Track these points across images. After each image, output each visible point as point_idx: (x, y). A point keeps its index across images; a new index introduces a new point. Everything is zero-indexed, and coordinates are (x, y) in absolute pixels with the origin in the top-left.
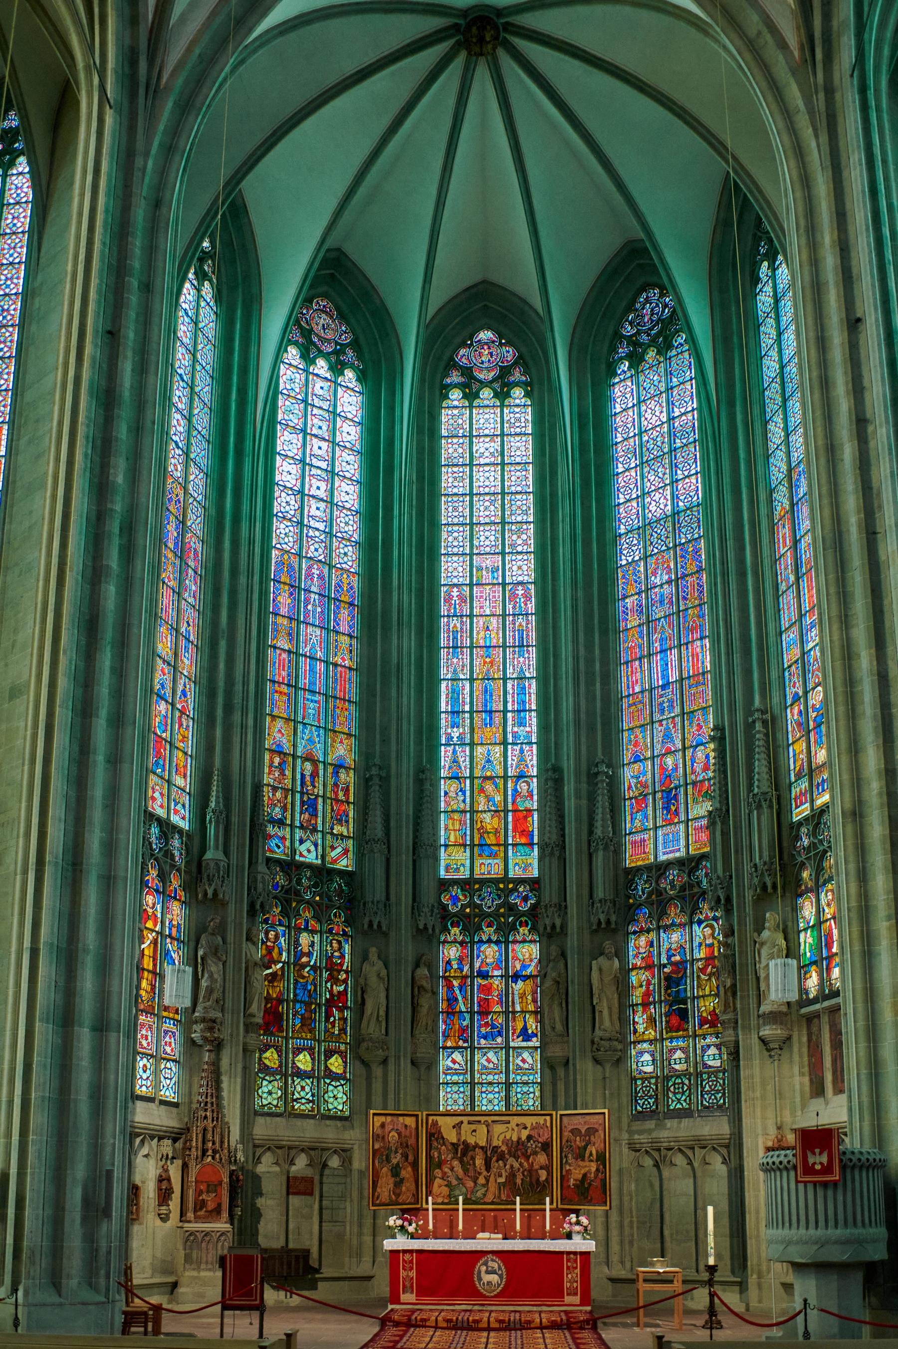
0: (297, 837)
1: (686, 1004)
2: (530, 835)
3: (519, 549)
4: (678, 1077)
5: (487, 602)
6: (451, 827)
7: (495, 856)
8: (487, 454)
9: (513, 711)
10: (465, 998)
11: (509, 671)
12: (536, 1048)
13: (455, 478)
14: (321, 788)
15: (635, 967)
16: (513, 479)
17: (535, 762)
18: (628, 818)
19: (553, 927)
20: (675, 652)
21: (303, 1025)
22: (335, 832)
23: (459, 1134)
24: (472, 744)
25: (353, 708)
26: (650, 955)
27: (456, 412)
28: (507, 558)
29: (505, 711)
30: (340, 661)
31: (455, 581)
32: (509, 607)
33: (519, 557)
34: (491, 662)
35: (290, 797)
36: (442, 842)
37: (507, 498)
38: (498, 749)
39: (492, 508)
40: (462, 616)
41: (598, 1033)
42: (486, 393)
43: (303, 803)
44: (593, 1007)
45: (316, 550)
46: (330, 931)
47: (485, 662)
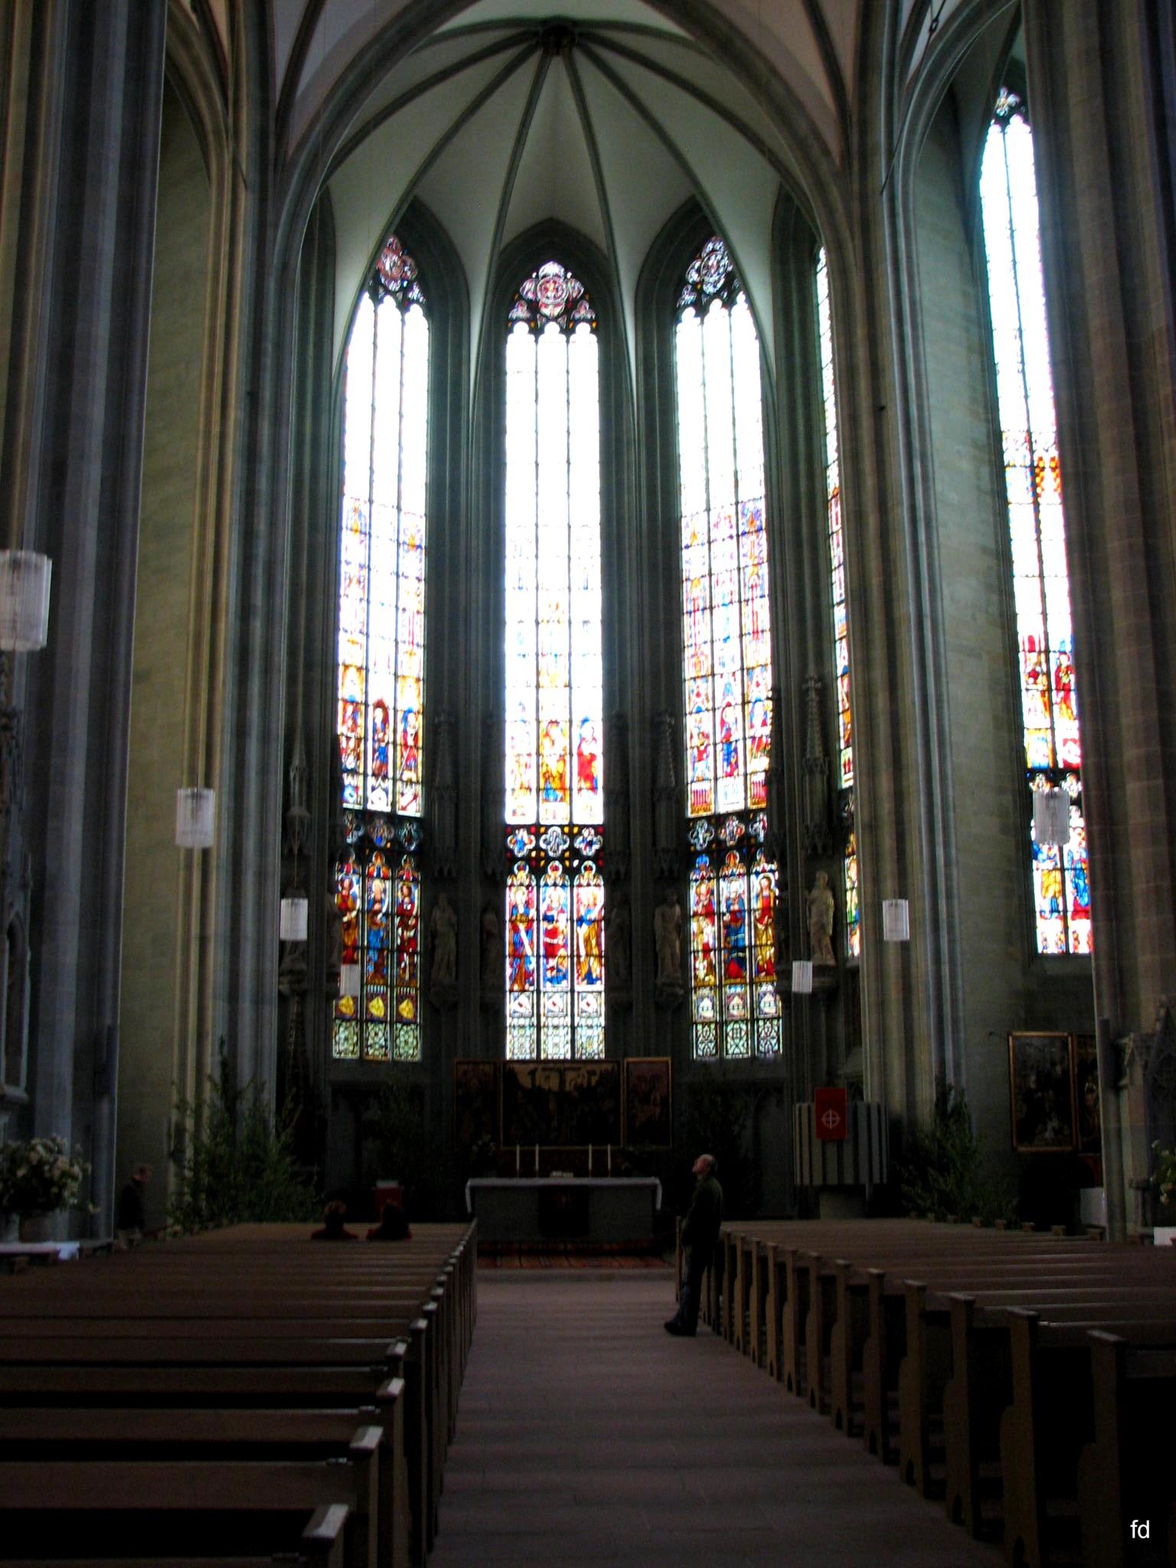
1: (744, 951)
4: (736, 1022)
10: (531, 943)
15: (696, 914)
19: (618, 873)
21: (376, 971)
23: (533, 1080)
26: (710, 903)
41: (659, 981)
42: (552, 329)
44: (656, 955)
46: (401, 878)
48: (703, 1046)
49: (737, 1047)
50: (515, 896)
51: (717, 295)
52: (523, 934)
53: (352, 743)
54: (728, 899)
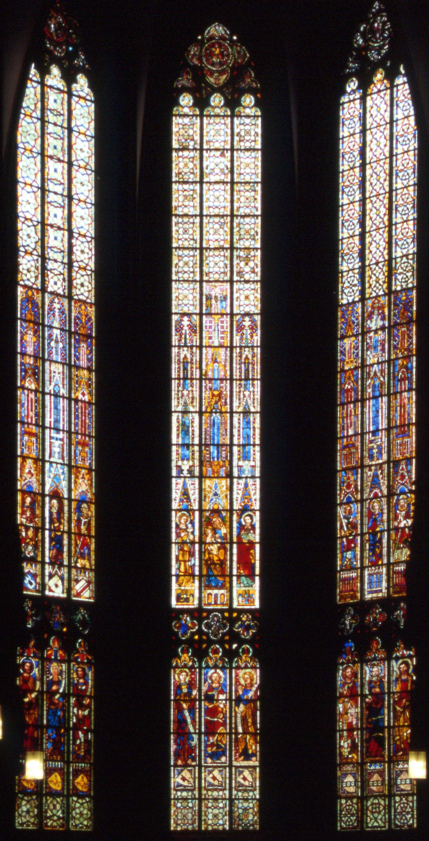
0: (47, 573)
1: (383, 733)
2: (253, 567)
3: (247, 277)
4: (375, 797)
5: (216, 331)
6: (181, 558)
7: (223, 587)
8: (217, 171)
9: (239, 445)
11: (236, 404)
12: (254, 767)
13: (186, 197)
14: (66, 524)
15: (342, 695)
16: (242, 199)
17: (258, 496)
18: (339, 556)
20: (385, 399)
22: (79, 565)
24: (201, 477)
25: (93, 443)
27: (186, 120)
28: (236, 286)
29: (231, 445)
30: (80, 397)
31: (186, 310)
32: (236, 339)
33: (247, 286)
34: (220, 395)
35: (40, 534)
36: (174, 572)
37: (236, 221)
38: (224, 483)
39: (221, 231)
40: (192, 347)
42: (217, 100)
43: (51, 540)
45: (56, 283)
47: (213, 395)
48: (346, 821)
49: (376, 821)
50: (180, 677)
51: (381, 64)
52: (187, 714)
53: (30, 533)
54: (370, 682)
